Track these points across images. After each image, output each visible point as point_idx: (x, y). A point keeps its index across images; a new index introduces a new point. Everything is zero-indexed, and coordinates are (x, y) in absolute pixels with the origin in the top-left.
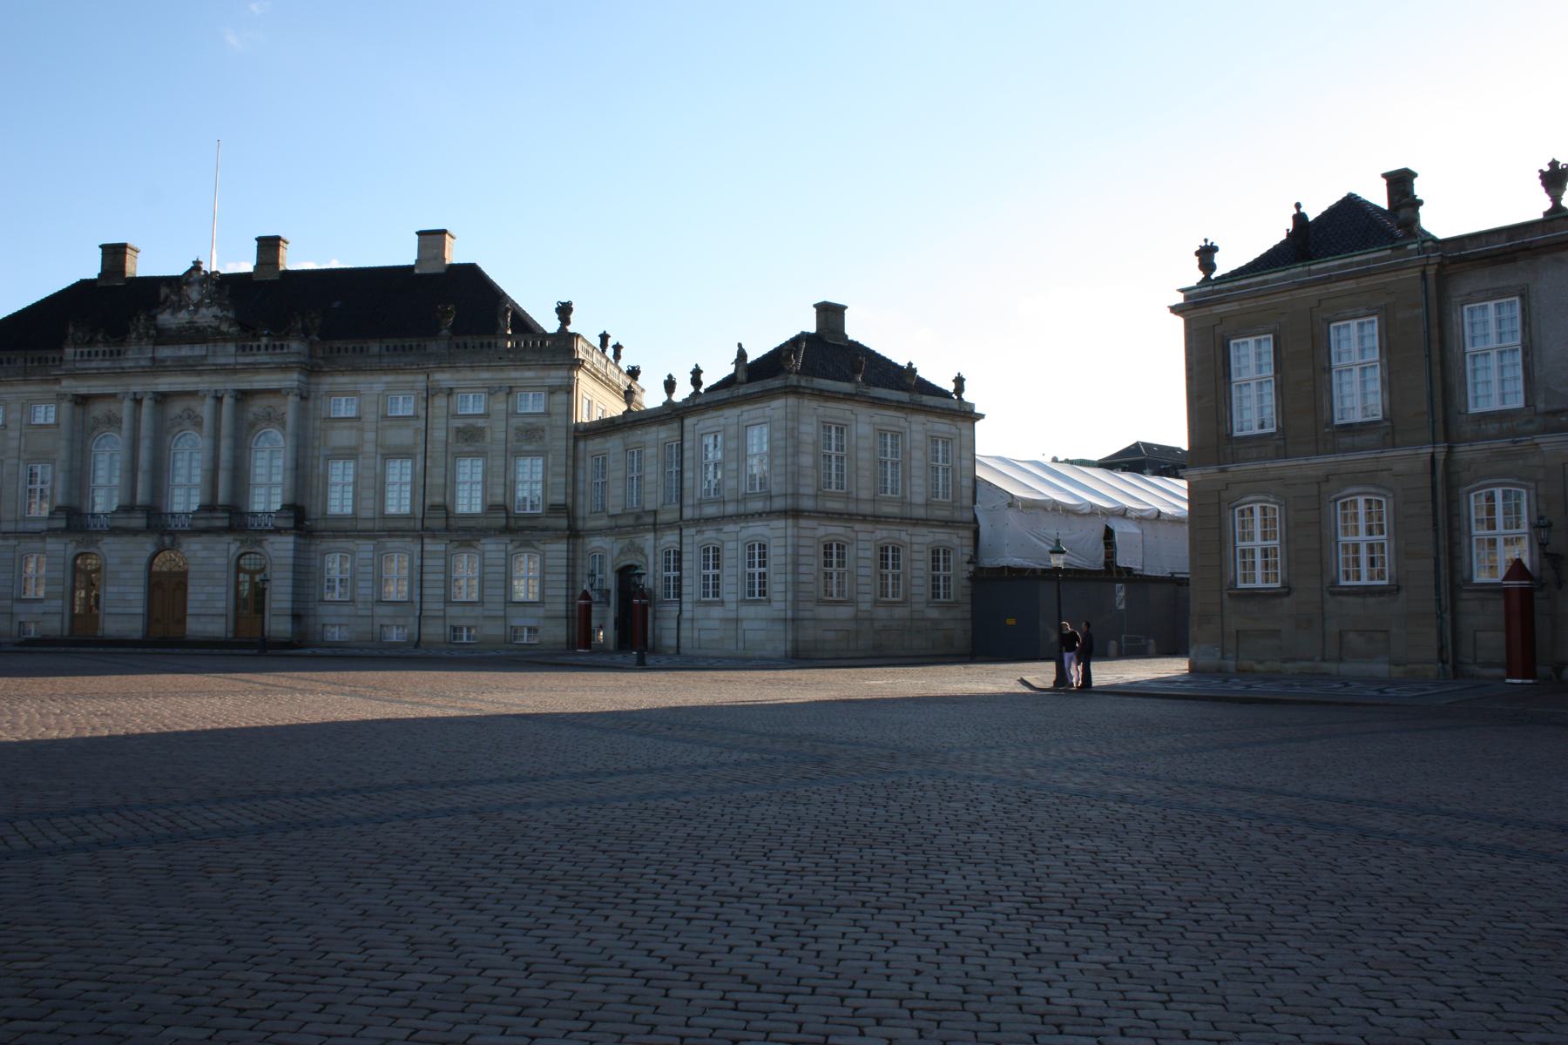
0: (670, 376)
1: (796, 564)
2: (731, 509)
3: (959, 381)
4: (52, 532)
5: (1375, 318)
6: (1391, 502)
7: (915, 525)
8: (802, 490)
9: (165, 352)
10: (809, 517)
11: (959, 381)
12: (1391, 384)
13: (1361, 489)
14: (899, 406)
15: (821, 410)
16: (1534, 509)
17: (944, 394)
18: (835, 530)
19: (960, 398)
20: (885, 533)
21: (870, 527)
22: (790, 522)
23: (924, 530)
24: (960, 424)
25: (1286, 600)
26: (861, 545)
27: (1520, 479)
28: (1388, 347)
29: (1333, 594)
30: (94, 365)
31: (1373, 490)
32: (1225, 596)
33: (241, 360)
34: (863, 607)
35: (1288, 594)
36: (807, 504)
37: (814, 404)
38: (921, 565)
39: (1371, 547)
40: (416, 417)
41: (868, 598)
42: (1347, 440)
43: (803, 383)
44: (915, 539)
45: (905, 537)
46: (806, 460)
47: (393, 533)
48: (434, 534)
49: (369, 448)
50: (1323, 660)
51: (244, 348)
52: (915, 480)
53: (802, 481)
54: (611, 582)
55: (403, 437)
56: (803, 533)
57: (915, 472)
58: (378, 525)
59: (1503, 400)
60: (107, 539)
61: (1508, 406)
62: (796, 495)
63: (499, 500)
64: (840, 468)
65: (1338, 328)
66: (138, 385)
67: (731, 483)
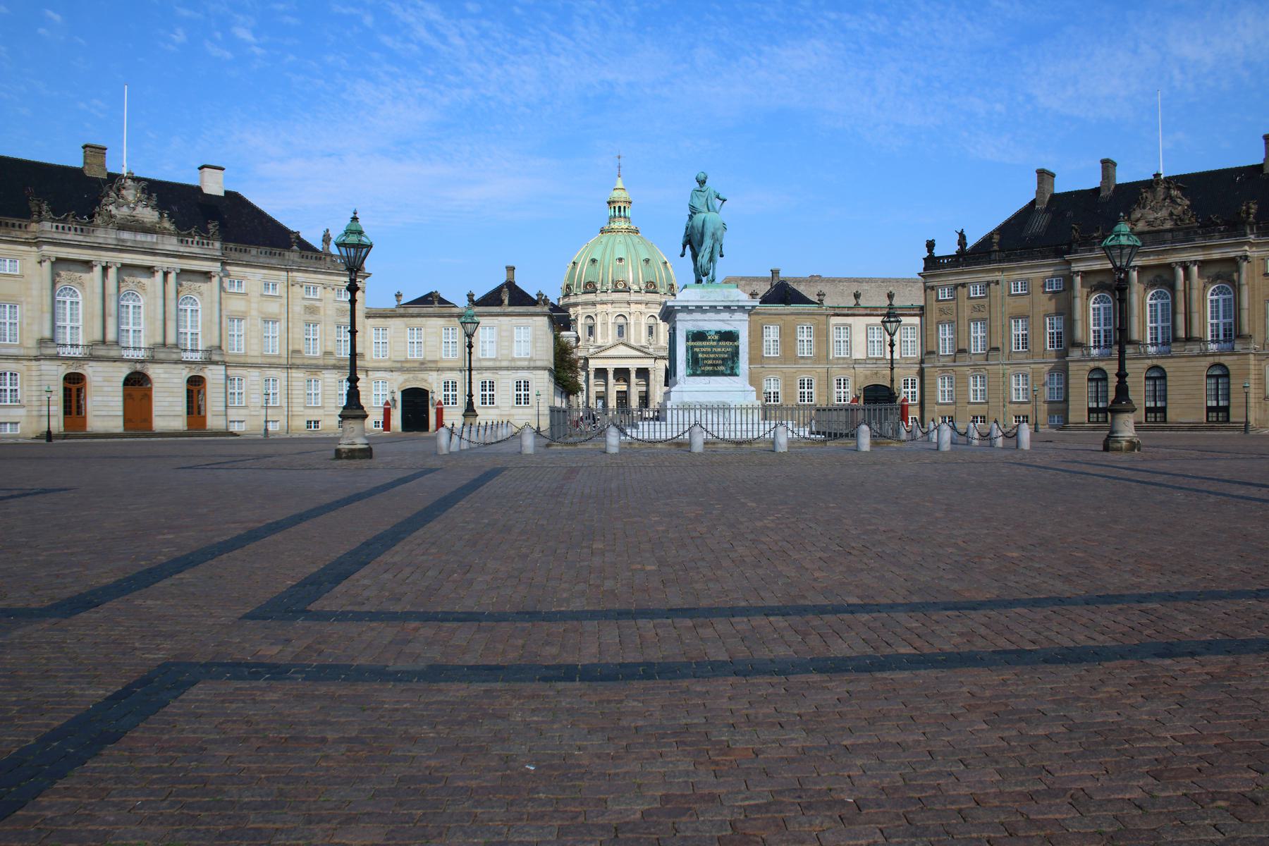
2: (505, 364)
9: (126, 235)
30: (69, 237)
33: (182, 249)
40: (280, 297)
47: (271, 366)
48: (298, 367)
49: (254, 313)
51: (182, 241)
54: (398, 397)
55: (274, 308)
58: (259, 361)
60: (91, 364)
63: (329, 349)
66: (106, 257)
67: (505, 352)
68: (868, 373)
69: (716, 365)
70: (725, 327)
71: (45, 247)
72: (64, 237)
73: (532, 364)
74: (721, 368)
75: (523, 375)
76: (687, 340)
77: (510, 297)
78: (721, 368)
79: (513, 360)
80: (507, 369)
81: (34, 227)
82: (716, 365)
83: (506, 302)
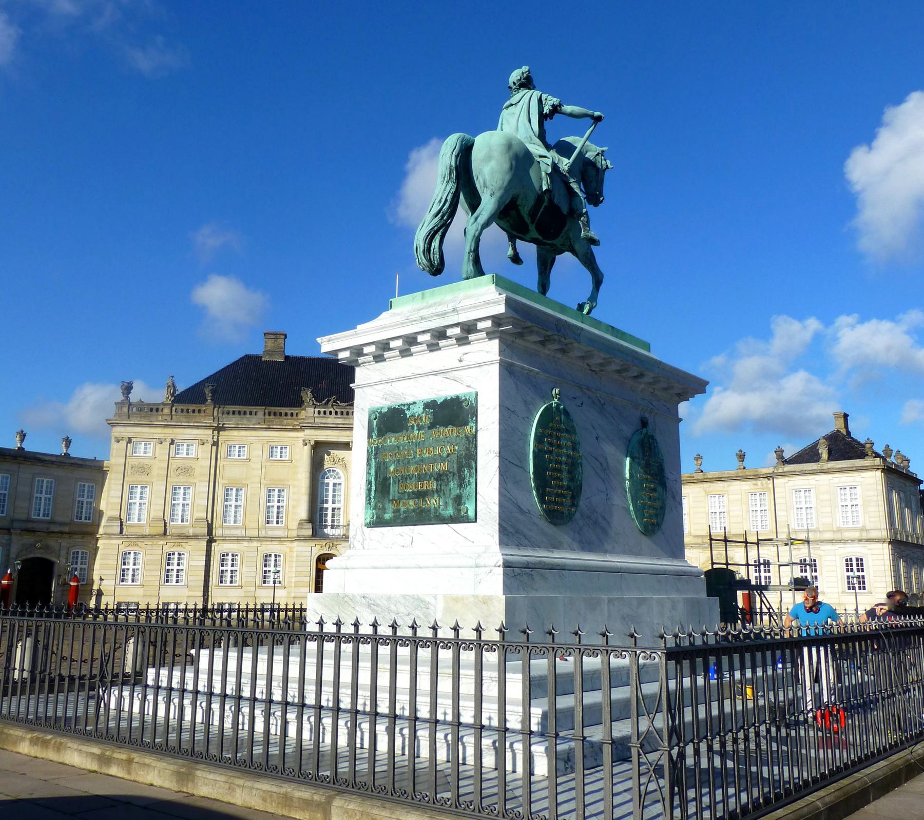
0: (741, 451)
4: (299, 538)
30: (329, 420)
69: (422, 495)
70: (443, 390)
71: (307, 432)
72: (324, 421)
73: (865, 535)
74: (432, 502)
75: (854, 551)
76: (370, 436)
77: (844, 448)
78: (432, 502)
79: (840, 530)
80: (831, 541)
81: (303, 414)
82: (422, 495)
83: (825, 455)
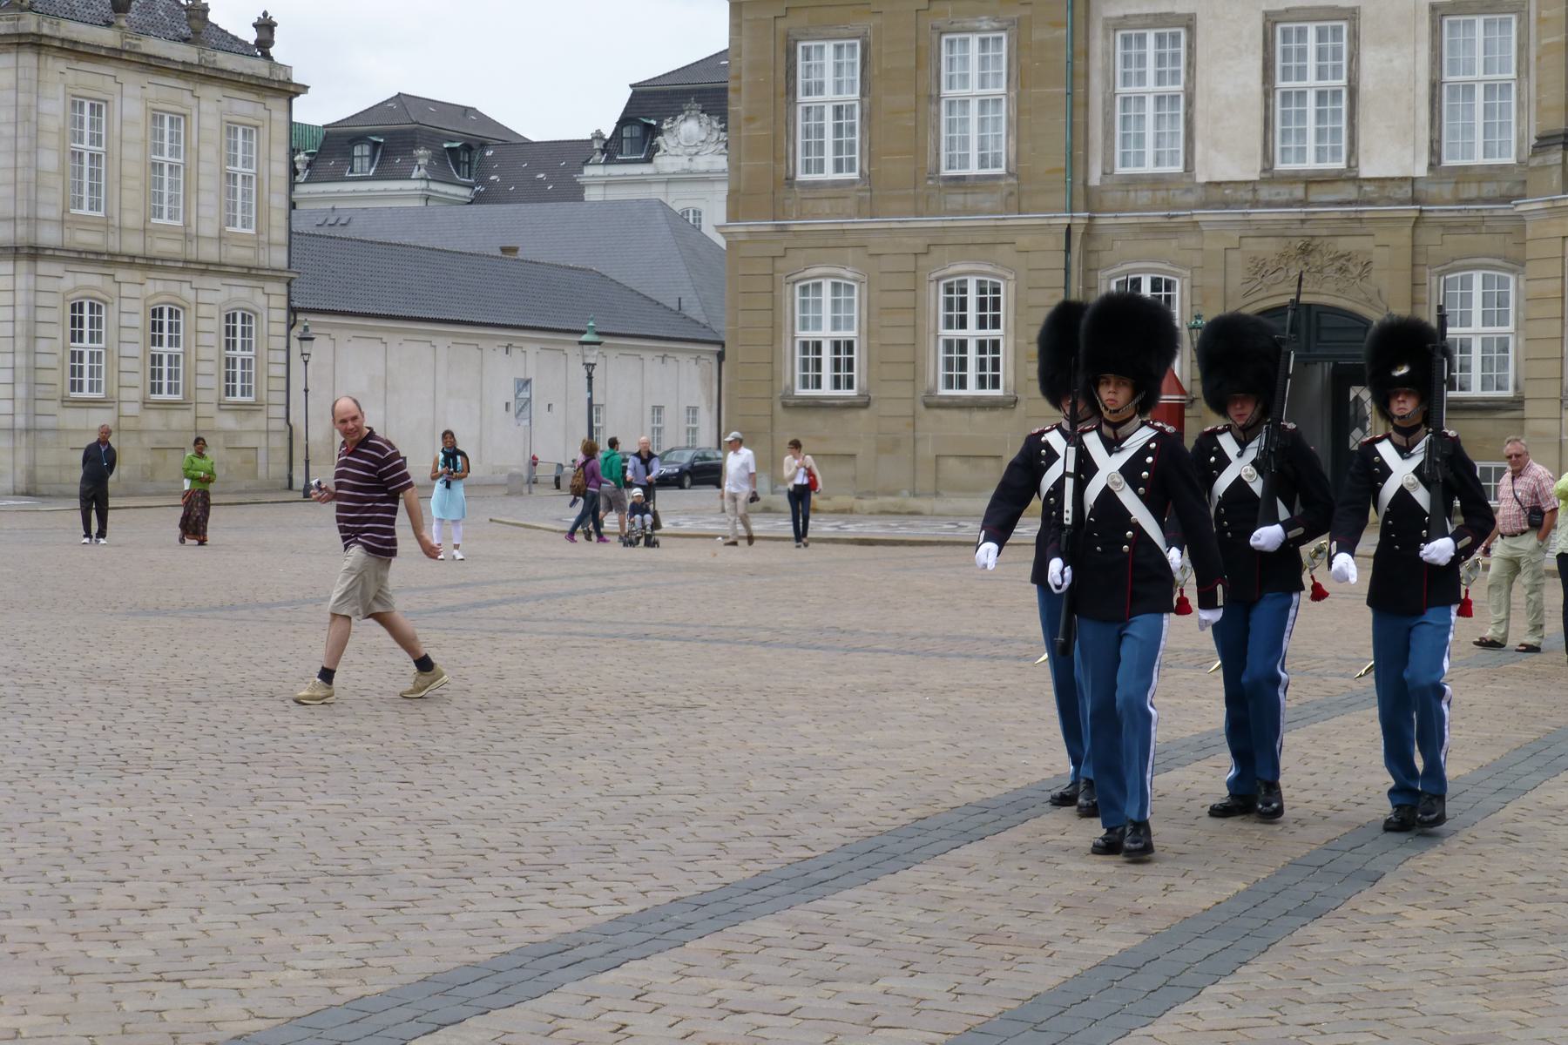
1: (33, 338)
3: (266, 26)
5: (1004, 35)
6: (1012, 285)
7: (204, 272)
8: (42, 213)
10: (53, 258)
11: (266, 26)
12: (1019, 126)
13: (972, 267)
14: (185, 72)
15: (70, 74)
16: (1187, 304)
17: (231, 43)
18: (87, 281)
19: (267, 56)
20: (160, 286)
21: (137, 275)
22: (23, 266)
23: (215, 282)
24: (270, 103)
25: (863, 413)
26: (203, 310)
27: (1173, 264)
28: (1020, 77)
29: (928, 406)
31: (988, 269)
32: (778, 407)
34: (128, 409)
35: (866, 405)
36: (48, 236)
37: (61, 65)
38: (137, 336)
39: (982, 347)
41: (135, 394)
42: (957, 199)
43: (46, 30)
44: (205, 296)
45: (187, 293)
46: (49, 160)
50: (914, 494)
52: (203, 197)
53: (42, 196)
56: (44, 284)
57: (204, 183)
59: (1158, 162)
61: (1166, 169)
62: (33, 220)
64: (95, 174)
65: (951, 43)
68: (1269, 248)
